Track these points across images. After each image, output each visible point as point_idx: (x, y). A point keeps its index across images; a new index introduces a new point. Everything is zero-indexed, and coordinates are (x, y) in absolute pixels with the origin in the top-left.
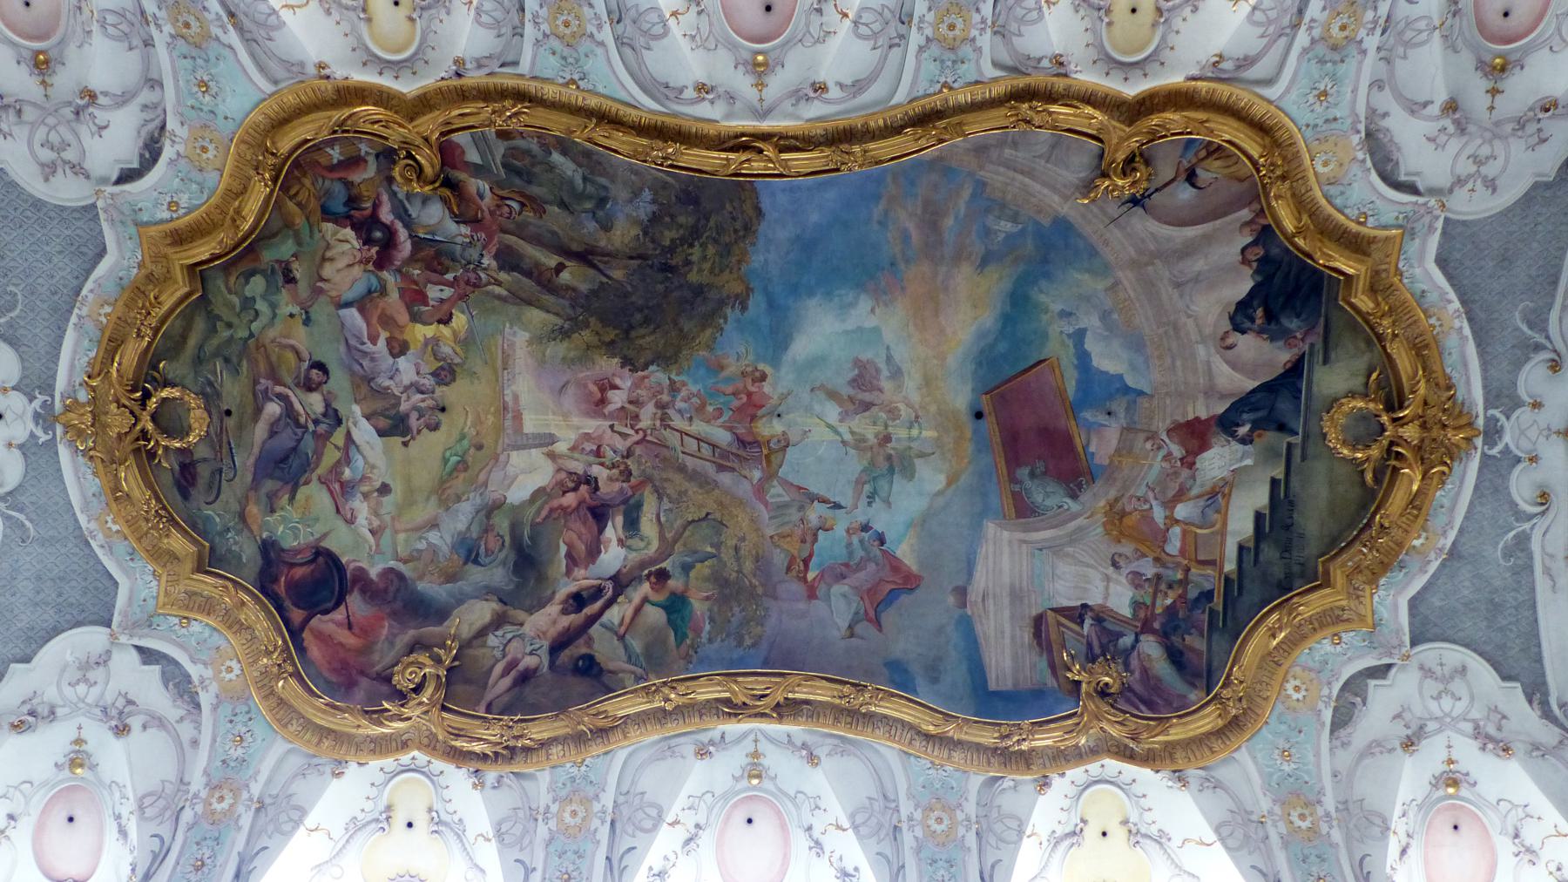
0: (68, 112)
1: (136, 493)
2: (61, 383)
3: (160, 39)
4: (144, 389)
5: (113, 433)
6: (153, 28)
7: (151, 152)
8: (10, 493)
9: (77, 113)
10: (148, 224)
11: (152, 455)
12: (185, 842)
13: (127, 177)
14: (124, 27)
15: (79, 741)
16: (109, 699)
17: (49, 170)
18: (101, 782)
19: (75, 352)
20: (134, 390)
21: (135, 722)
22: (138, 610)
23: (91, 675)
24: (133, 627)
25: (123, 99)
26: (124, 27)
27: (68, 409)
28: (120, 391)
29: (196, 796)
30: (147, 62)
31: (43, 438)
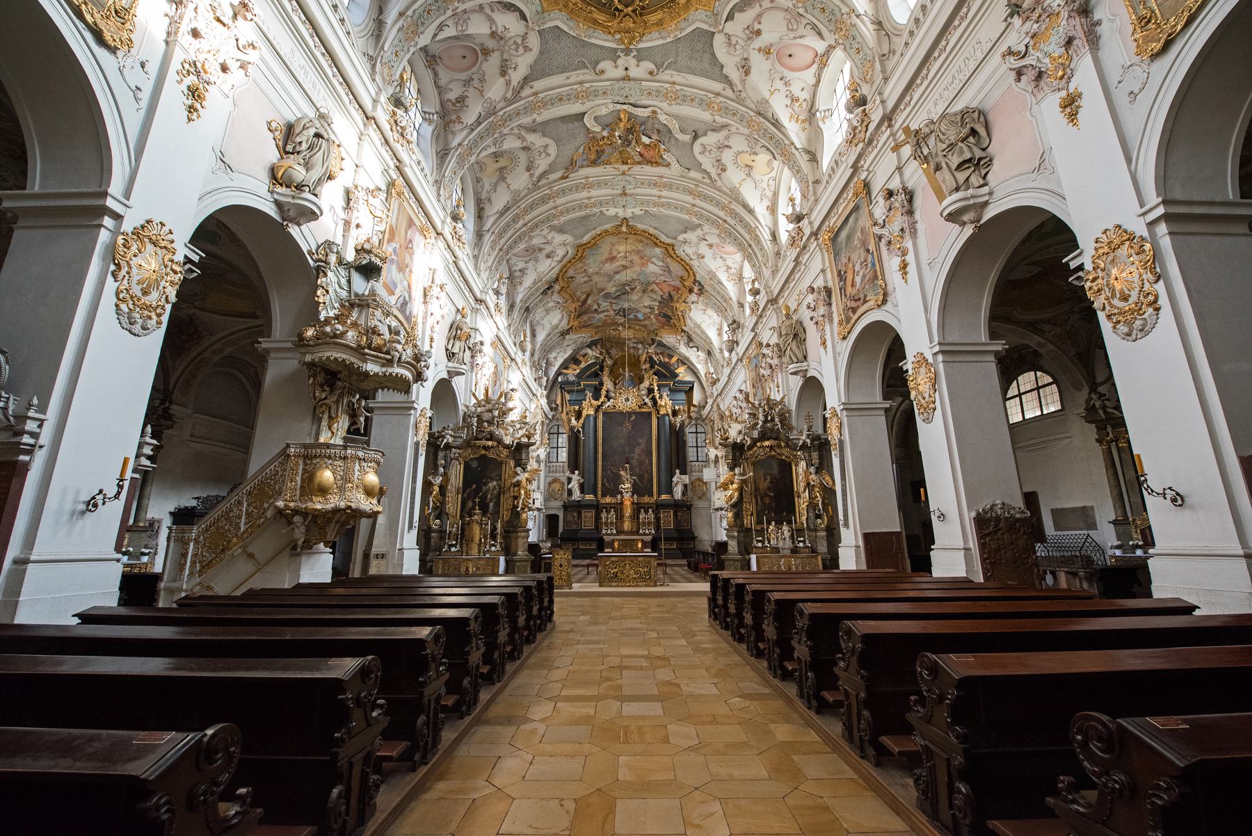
0: (502, 42)
1: (659, 16)
2: (613, 45)
3: (462, 7)
4: (615, 10)
5: (632, 25)
6: (458, 11)
7: (511, 7)
8: (656, 67)
9: (502, 38)
10: (542, 8)
11: (643, 8)
12: (812, 15)
13: (523, 17)
14: (461, 22)
15: (760, 50)
16: (744, 36)
17: (527, 49)
18: (779, 43)
19: (600, 39)
20: (615, 15)
21: (757, 27)
22: (709, 20)
23: (733, 42)
24: (717, 23)
25: (492, 21)
26: (461, 22)
27: (623, 43)
28: (615, 22)
29: (794, 5)
30: (473, 11)
31: (635, 53)
